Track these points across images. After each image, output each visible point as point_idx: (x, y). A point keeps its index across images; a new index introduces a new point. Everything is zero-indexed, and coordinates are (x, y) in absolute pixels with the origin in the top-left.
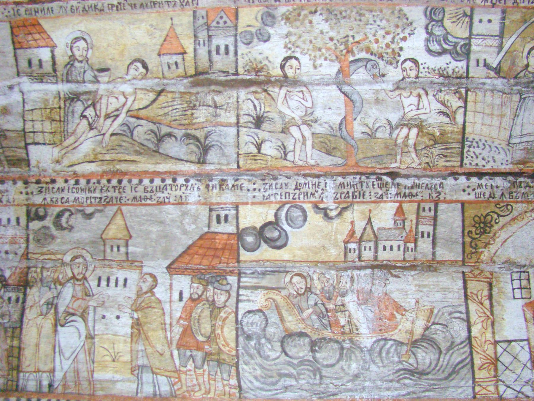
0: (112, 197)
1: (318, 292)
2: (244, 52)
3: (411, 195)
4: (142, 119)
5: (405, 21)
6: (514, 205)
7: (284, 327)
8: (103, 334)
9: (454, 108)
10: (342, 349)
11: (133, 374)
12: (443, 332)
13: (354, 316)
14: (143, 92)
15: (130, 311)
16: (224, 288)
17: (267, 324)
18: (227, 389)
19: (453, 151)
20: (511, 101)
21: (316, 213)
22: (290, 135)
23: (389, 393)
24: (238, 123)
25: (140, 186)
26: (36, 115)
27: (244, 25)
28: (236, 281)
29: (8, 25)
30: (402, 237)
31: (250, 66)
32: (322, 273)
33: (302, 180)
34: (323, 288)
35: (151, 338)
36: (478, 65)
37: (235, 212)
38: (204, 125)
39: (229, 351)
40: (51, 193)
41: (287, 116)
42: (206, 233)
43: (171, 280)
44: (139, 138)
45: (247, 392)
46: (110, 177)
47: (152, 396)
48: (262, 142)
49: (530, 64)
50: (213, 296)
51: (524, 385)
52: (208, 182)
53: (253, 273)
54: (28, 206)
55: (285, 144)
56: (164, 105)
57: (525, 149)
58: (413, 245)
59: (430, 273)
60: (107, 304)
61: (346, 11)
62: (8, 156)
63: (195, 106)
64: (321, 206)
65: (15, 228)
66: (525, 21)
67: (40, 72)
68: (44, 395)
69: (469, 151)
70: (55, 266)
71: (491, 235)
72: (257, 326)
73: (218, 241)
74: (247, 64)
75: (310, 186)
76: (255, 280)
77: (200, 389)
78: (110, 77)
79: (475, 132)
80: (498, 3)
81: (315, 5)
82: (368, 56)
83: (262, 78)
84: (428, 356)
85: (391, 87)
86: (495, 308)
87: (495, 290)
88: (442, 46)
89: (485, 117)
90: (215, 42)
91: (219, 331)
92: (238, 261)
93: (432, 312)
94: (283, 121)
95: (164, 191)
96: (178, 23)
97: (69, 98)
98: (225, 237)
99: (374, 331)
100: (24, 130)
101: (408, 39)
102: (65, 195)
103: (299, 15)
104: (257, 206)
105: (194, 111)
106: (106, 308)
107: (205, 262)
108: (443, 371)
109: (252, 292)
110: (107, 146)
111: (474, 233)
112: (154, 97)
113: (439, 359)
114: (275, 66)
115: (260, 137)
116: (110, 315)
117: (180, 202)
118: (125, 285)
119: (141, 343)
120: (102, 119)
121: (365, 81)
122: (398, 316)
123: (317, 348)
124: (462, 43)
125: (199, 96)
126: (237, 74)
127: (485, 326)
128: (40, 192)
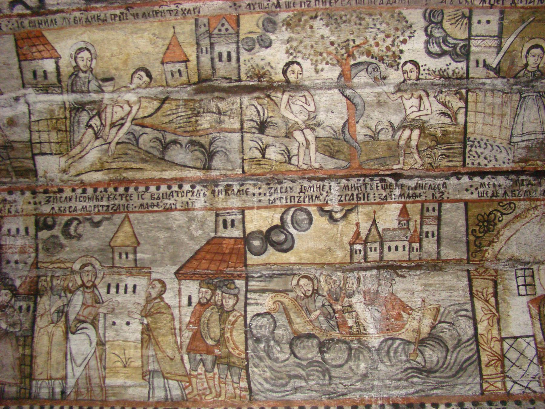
0: (119, 205)
1: (325, 294)
2: (246, 59)
3: (415, 196)
4: (147, 127)
5: (404, 23)
6: (517, 203)
7: (292, 329)
8: (114, 341)
9: (455, 109)
10: (350, 349)
11: (145, 380)
12: (449, 330)
13: (362, 316)
14: (148, 100)
15: (139, 317)
16: (232, 292)
17: (275, 327)
18: (238, 391)
19: (455, 151)
20: (512, 100)
22: (293, 139)
23: (398, 392)
24: (242, 128)
25: (147, 194)
26: (42, 126)
27: (246, 31)
28: (244, 285)
29: (12, 38)
30: (407, 237)
31: (253, 72)
32: (329, 275)
33: (306, 184)
34: (330, 290)
35: (161, 343)
36: (477, 66)
37: (241, 216)
38: (209, 132)
39: (238, 354)
41: (290, 121)
43: (179, 285)
44: (145, 145)
45: (258, 394)
47: (163, 400)
48: (266, 147)
49: (529, 63)
50: (222, 300)
51: (531, 381)
52: (214, 188)
53: (260, 277)
54: (36, 215)
56: (169, 113)
57: (526, 147)
58: (417, 245)
59: (436, 272)
60: (116, 311)
61: (346, 15)
62: (16, 167)
63: (199, 112)
64: (326, 208)
65: (24, 238)
66: (523, 21)
67: (45, 83)
68: (57, 402)
69: (470, 151)
70: (65, 275)
71: (495, 233)
72: (265, 328)
73: (225, 246)
74: (249, 71)
75: (315, 189)
76: (263, 284)
77: (211, 393)
78: (114, 86)
79: (477, 132)
80: (496, 4)
81: (315, 10)
82: (369, 59)
83: (265, 84)
84: (435, 355)
85: (392, 89)
86: (500, 305)
87: (500, 287)
88: (441, 47)
89: (486, 117)
90: (217, 49)
91: (228, 335)
92: (246, 265)
93: (438, 310)
94: (287, 125)
95: (171, 197)
96: (181, 31)
97: (75, 108)
98: (232, 241)
99: (382, 331)
100: (30, 140)
102: (73, 204)
103: (300, 20)
104: (263, 210)
105: (198, 118)
107: (213, 266)
108: (451, 369)
109: (260, 296)
110: (113, 154)
111: (478, 232)
112: (159, 105)
113: (446, 357)
114: (277, 71)
115: (264, 141)
117: (187, 208)
118: (134, 291)
119: (152, 348)
120: (107, 128)
121: (367, 85)
122: (405, 316)
123: (325, 349)
124: (461, 44)
125: (202, 103)
126: (240, 80)
127: (491, 323)
128: (48, 201)
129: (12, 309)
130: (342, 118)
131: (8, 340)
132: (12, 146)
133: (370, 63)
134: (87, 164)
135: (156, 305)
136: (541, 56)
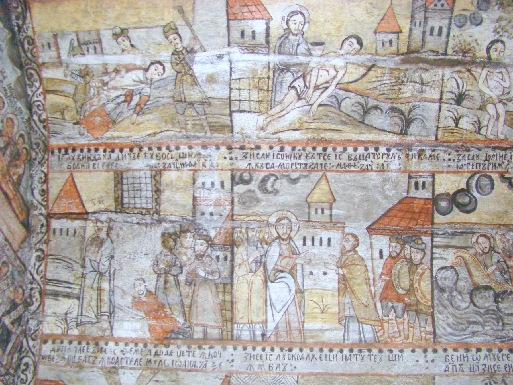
0: (317, 164)
1: (500, 251)
7: (472, 281)
8: (312, 289)
15: (335, 268)
17: (458, 279)
21: (502, 182)
22: (485, 112)
25: (344, 154)
26: (243, 85)
27: (461, 8)
28: (430, 241)
32: (503, 235)
33: (491, 152)
34: (504, 248)
35: (357, 292)
37: (431, 179)
38: (410, 100)
39: (425, 302)
40: (256, 158)
41: (486, 95)
42: (405, 198)
43: (370, 239)
44: (346, 109)
45: (441, 337)
46: (315, 144)
48: (460, 118)
54: (232, 170)
55: (481, 120)
56: (374, 80)
60: (313, 262)
63: (403, 82)
64: (507, 176)
65: (219, 191)
67: (252, 43)
68: (258, 343)
70: (260, 227)
74: (456, 46)
75: (498, 158)
76: (446, 240)
77: (400, 336)
83: (468, 59)
90: (430, 23)
91: (416, 285)
92: (433, 223)
96: (398, 3)
97: (279, 69)
98: (422, 202)
100: (230, 98)
102: (270, 161)
105: (402, 87)
106: (313, 265)
107: (403, 224)
109: (444, 251)
110: (314, 115)
112: (365, 71)
114: (482, 48)
115: (459, 112)
116: (318, 272)
118: (329, 244)
119: (348, 296)
120: (311, 90)
123: (500, 300)
125: (407, 73)
126: (446, 54)
128: (245, 157)
129: (208, 258)
131: (207, 287)
132: (209, 102)
134: (287, 123)
135: (349, 257)
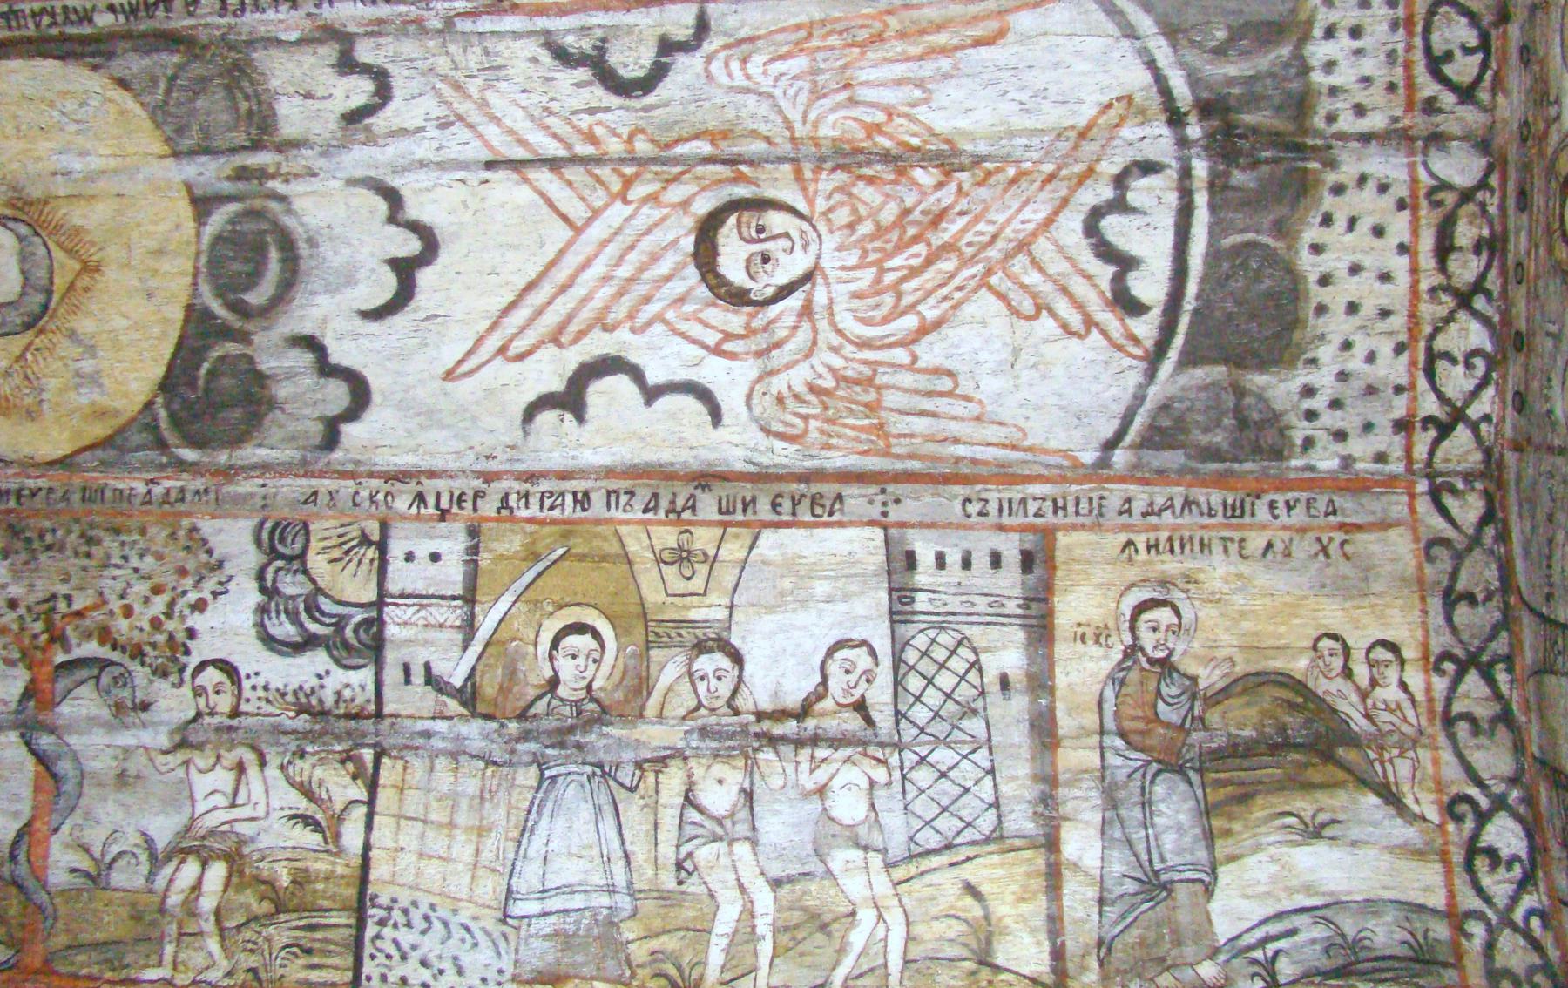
5: (204, 557)
9: (338, 806)
19: (330, 935)
20: (513, 786)
36: (408, 681)
49: (561, 675)
57: (556, 933)
66: (535, 557)
69: (378, 937)
79: (401, 880)
80: (455, 510)
82: (105, 652)
85: (164, 741)
88: (301, 625)
89: (431, 834)
101: (210, 608)
121: (93, 721)
124: (358, 618)
130: (16, 814)
133: (108, 663)
136: (596, 655)
